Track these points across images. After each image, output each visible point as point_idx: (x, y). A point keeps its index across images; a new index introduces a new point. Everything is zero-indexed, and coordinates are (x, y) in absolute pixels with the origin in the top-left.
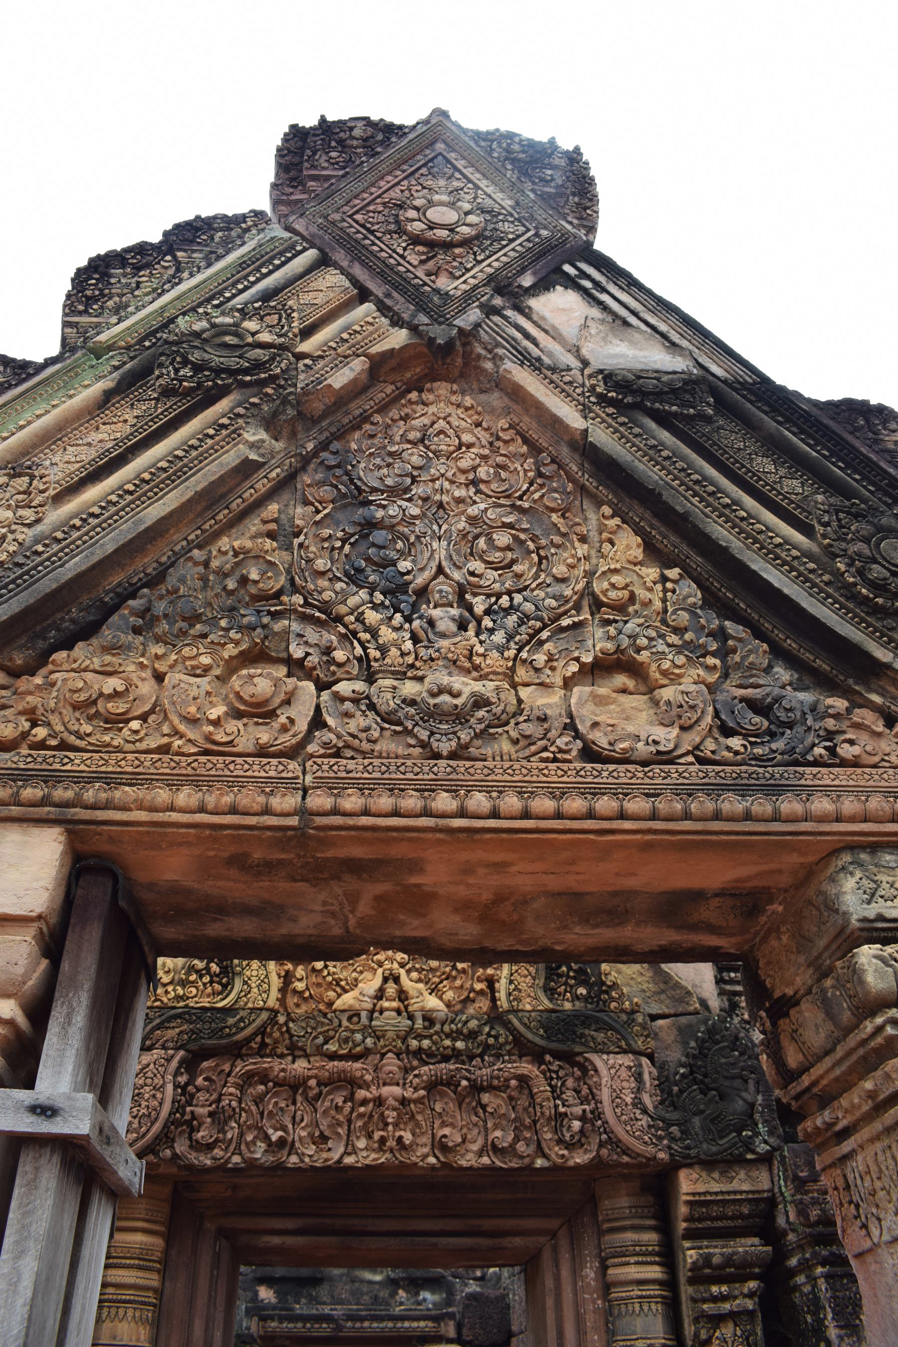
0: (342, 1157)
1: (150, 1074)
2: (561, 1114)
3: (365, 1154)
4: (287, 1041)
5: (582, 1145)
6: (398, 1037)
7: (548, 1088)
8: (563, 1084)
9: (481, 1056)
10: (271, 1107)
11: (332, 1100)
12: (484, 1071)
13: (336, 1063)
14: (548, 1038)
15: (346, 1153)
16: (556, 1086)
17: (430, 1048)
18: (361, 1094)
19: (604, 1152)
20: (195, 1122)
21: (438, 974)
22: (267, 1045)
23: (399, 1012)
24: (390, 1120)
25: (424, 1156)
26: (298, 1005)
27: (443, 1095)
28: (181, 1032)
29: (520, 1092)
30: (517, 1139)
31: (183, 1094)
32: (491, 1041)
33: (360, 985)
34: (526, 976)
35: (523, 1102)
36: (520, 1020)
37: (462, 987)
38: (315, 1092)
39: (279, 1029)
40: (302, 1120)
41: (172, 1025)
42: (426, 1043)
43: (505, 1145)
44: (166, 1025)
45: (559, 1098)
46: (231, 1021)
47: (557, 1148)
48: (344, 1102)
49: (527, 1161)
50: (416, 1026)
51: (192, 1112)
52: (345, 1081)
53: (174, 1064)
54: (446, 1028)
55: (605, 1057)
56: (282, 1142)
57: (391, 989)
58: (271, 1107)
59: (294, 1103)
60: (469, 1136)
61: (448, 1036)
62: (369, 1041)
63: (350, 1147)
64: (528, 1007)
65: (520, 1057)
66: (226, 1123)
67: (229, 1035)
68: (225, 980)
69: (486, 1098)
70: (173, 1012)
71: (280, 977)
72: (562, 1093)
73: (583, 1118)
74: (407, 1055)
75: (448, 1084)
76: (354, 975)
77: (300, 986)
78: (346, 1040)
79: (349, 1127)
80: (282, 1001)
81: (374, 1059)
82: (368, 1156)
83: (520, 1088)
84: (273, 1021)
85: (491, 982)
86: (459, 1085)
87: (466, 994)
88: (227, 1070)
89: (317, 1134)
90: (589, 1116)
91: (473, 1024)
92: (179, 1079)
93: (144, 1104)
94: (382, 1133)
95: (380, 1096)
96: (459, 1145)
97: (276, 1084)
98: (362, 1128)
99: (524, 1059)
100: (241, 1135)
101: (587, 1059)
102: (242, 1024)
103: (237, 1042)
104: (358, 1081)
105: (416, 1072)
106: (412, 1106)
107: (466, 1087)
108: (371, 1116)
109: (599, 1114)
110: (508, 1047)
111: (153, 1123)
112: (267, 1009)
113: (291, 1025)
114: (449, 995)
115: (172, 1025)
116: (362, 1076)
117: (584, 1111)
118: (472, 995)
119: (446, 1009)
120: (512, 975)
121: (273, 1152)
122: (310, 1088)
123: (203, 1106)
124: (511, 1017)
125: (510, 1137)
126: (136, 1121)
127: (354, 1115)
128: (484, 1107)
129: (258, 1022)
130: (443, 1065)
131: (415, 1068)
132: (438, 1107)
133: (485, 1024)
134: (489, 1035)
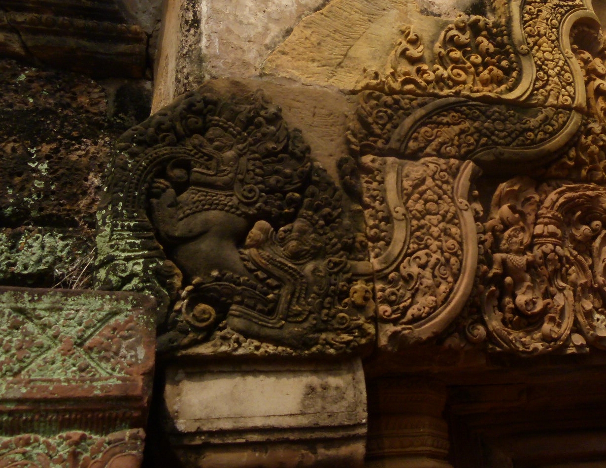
1: (429, 195)
20: (508, 279)
28: (462, 132)
51: (504, 262)
67: (533, 142)
93: (434, 245)
111: (456, 277)
115: (445, 120)
126: (428, 273)
129: (571, 127)
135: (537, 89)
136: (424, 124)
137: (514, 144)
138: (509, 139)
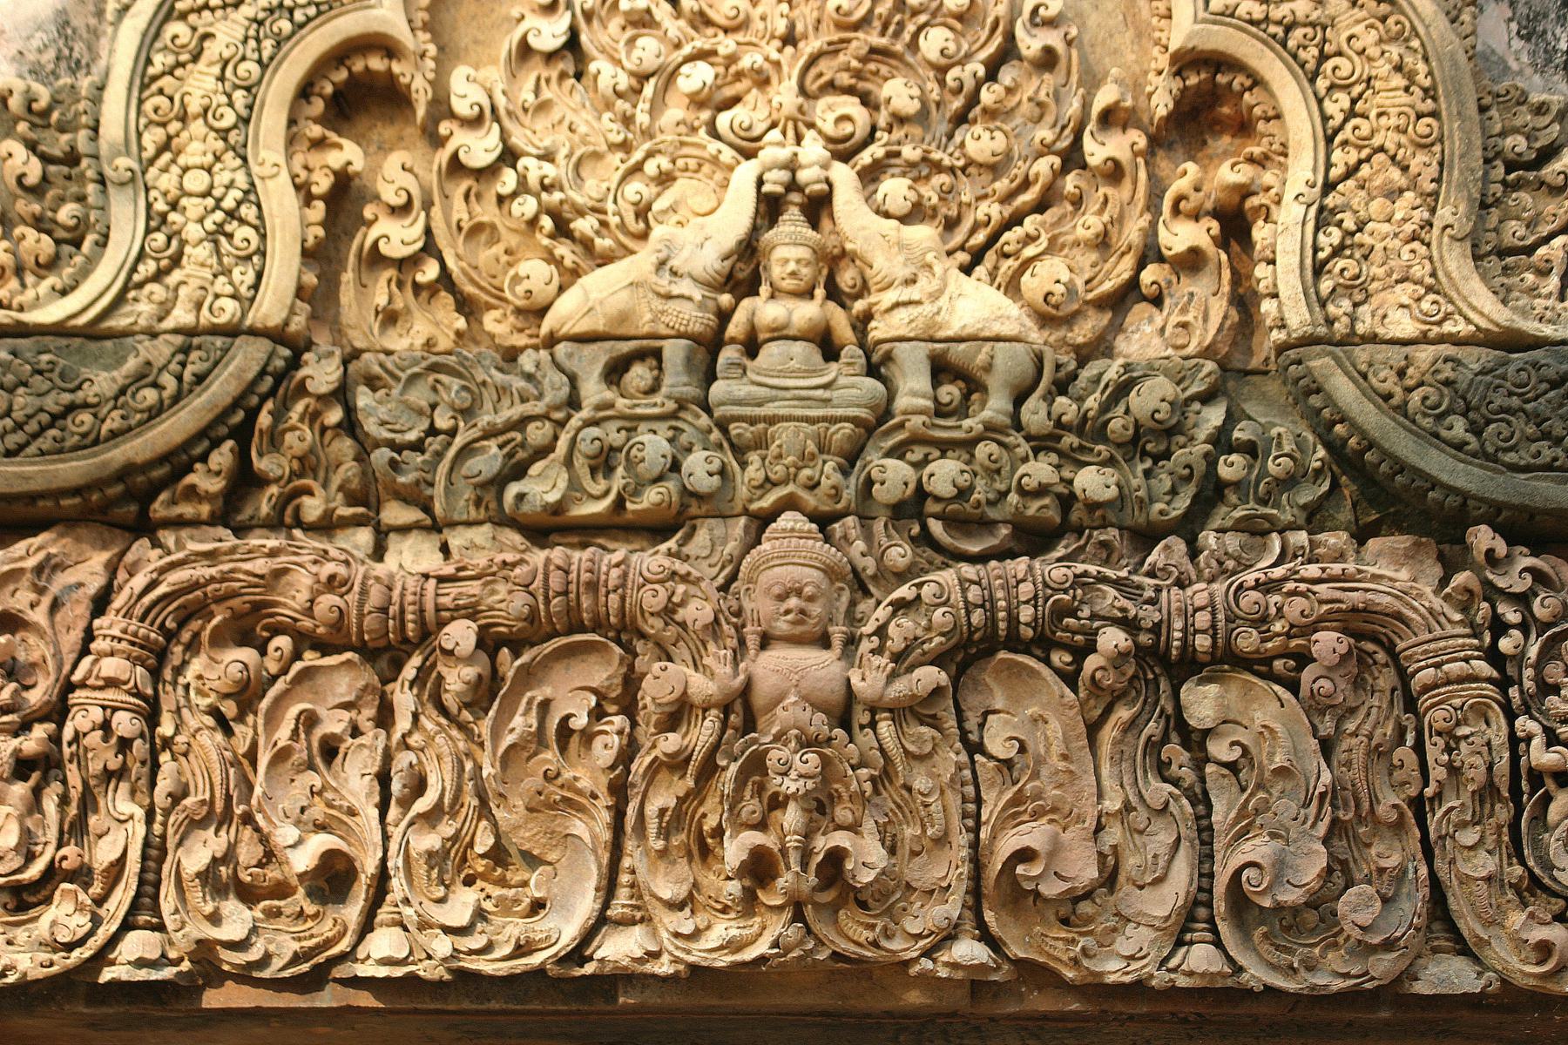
0: (589, 935)
2: (1536, 777)
4: (348, 470)
6: (823, 448)
7: (1483, 667)
9: (1189, 527)
10: (283, 735)
11: (545, 705)
12: (1199, 593)
13: (557, 554)
14: (1487, 457)
15: (601, 922)
16: (1519, 658)
17: (963, 493)
18: (662, 681)
21: (1002, 185)
22: (262, 482)
23: (829, 348)
24: (790, 785)
26: (390, 318)
29: (1358, 683)
30: (1339, 873)
32: (1231, 467)
33: (658, 232)
34: (1394, 194)
35: (1374, 718)
37: (1102, 243)
38: (470, 672)
39: (313, 417)
40: (419, 786)
42: (945, 473)
43: (1290, 896)
47: (1516, 919)
48: (598, 714)
49: (1383, 966)
50: (902, 402)
52: (598, 625)
54: (1035, 413)
56: (332, 878)
57: (789, 248)
59: (385, 717)
60: (1131, 863)
61: (1042, 444)
62: (699, 468)
63: (623, 896)
64: (1404, 326)
65: (1361, 536)
68: (67, 213)
69: (1202, 702)
71: (309, 200)
74: (865, 519)
75: (1042, 645)
76: (635, 189)
77: (398, 237)
78: (603, 462)
79: (619, 814)
80: (319, 297)
81: (712, 541)
82: (696, 935)
83: (1357, 666)
84: (280, 382)
85: (1235, 222)
86: (1091, 648)
87: (1123, 270)
88: (95, 584)
91: (1149, 398)
94: (754, 838)
95: (747, 690)
96: (1088, 895)
97: (304, 641)
98: (674, 820)
99: (1373, 544)
100: (154, 852)
102: (150, 396)
103: (127, 471)
104: (653, 626)
105: (905, 591)
106: (885, 728)
107: (1120, 658)
108: (709, 769)
110: (1307, 495)
112: (253, 332)
113: (364, 399)
114: (1048, 276)
116: (669, 611)
118: (1149, 275)
119: (1036, 336)
120: (1329, 187)
124: (1320, 363)
125: (1311, 866)
127: (640, 765)
128: (1195, 740)
129: (222, 387)
130: (1020, 565)
131: (902, 577)
132: (998, 742)
133: (1207, 398)
134: (1222, 441)
135: (140, 286)
137: (32, 449)
138: (19, 437)
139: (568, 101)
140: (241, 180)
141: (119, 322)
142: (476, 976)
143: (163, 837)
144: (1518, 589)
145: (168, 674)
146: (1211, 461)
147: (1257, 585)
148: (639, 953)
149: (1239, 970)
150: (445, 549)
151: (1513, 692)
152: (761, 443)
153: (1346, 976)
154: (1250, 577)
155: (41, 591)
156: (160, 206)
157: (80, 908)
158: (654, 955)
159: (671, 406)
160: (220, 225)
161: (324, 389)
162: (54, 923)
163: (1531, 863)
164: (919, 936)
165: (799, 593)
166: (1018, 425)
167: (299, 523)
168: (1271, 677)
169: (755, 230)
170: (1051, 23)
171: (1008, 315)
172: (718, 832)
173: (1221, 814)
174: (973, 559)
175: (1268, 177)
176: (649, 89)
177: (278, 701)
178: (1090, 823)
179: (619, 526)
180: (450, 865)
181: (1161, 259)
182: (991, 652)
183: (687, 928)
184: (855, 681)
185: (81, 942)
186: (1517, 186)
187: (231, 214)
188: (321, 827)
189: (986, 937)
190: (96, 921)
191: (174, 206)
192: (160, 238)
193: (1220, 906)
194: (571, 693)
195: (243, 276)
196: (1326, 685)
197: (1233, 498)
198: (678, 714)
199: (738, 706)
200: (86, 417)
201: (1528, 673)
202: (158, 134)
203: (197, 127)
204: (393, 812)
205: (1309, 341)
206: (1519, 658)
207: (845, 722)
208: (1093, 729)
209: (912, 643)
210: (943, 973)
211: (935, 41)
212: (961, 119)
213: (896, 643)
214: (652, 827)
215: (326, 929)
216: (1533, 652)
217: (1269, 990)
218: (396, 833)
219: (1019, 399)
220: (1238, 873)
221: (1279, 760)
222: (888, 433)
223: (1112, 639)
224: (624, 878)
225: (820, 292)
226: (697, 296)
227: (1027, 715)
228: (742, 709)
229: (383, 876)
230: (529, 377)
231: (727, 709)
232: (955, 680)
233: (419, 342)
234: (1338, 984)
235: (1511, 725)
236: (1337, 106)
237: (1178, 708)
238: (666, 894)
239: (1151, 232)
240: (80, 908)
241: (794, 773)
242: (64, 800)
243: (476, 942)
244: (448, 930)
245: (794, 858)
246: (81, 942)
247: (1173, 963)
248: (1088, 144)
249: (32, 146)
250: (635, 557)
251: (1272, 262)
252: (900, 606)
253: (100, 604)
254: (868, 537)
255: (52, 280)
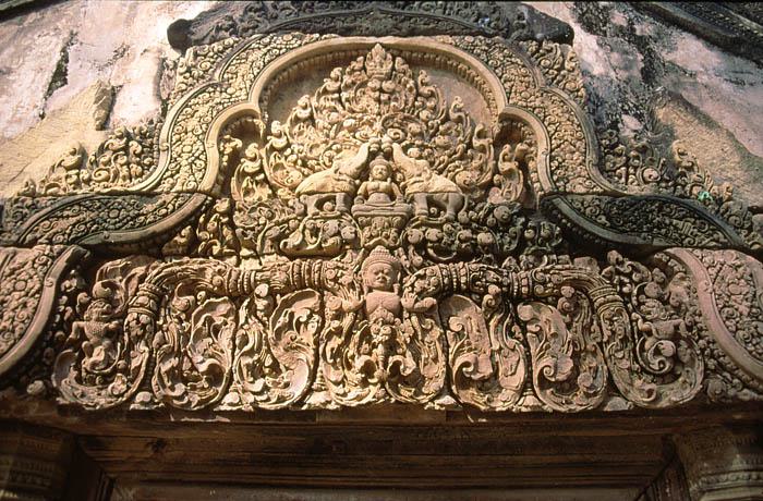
1: (24, 276)
2: (640, 333)
3: (340, 390)
5: (677, 377)
8: (641, 291)
9: (516, 254)
10: (199, 324)
11: (292, 315)
12: (523, 274)
14: (613, 227)
15: (309, 391)
19: (715, 384)
23: (392, 196)
25: (433, 398)
26: (248, 192)
27: (462, 306)
28: (78, 222)
31: (72, 302)
32: (528, 234)
36: (570, 204)
37: (481, 169)
38: (265, 302)
41: (66, 213)
42: (433, 234)
43: (560, 377)
44: (59, 214)
45: (637, 308)
46: (149, 207)
47: (638, 383)
48: (310, 317)
53: (61, 263)
54: (462, 215)
55: (698, 252)
56: (215, 374)
57: (378, 166)
58: (199, 324)
61: (466, 226)
62: (347, 232)
66: (131, 346)
69: (525, 311)
70: (72, 198)
72: (640, 304)
73: (675, 337)
75: (468, 292)
78: (315, 232)
79: (316, 350)
80: (223, 187)
82: (345, 395)
84: (209, 209)
86: (486, 292)
87: (488, 177)
89: (269, 362)
90: (683, 332)
91: (499, 213)
92: (67, 283)
94: (365, 358)
96: (488, 380)
97: (210, 294)
98: (337, 353)
99: (576, 260)
100: (151, 363)
101: (673, 257)
102: (164, 211)
103: (154, 235)
104: (330, 284)
105: (421, 272)
107: (496, 296)
108: (349, 335)
109: (701, 330)
112: (200, 192)
115: (66, 213)
116: (335, 279)
117: (677, 327)
118: (496, 177)
120: (552, 151)
121: (203, 389)
122: (258, 296)
123: (98, 320)
125: (567, 366)
127: (325, 332)
128: (523, 326)
129: (188, 208)
133: (519, 215)
134: (525, 225)
136: (47, 219)
138: (120, 224)
139: (309, 131)
140: (201, 148)
141: (159, 190)
142: (264, 410)
143: (155, 359)
144: (628, 271)
145: (163, 304)
146: (522, 231)
147: (542, 271)
148: (323, 401)
149: (544, 404)
150: (260, 264)
151: (629, 305)
152: (369, 224)
153: (581, 405)
154: (539, 269)
155: (124, 277)
156: (175, 156)
157: (123, 382)
158: (330, 402)
159: (339, 213)
160: (193, 162)
161: (222, 210)
162: (113, 388)
163: (641, 363)
164: (427, 395)
165: (383, 272)
166: (456, 219)
167: (212, 255)
168: (547, 303)
169: (368, 162)
170: (460, 110)
171: (453, 187)
172: (353, 357)
173: (533, 350)
174: (445, 262)
175: (532, 149)
176: (334, 127)
177: (198, 313)
178: (488, 353)
179: (322, 254)
180: (256, 371)
181: (499, 173)
182: (450, 295)
183: (341, 392)
184: (403, 302)
185: (122, 395)
186: (609, 153)
187: (198, 158)
188: (211, 357)
189: (452, 395)
190: (128, 388)
191: (179, 156)
192: (174, 165)
193: (536, 382)
194: (301, 310)
195: (198, 175)
196: (567, 304)
197: (529, 243)
198: (339, 315)
199: (360, 312)
200: (143, 218)
201: (634, 299)
202: (178, 136)
203: (190, 134)
204: (237, 351)
205: (551, 194)
206: (629, 295)
207: (400, 316)
208: (487, 322)
209: (424, 289)
210: (437, 408)
211: (424, 114)
212: (434, 135)
213: (417, 289)
214: (328, 355)
215: (211, 393)
216: (635, 292)
217: (555, 412)
218: (236, 358)
219: (457, 212)
220: (542, 370)
221: (553, 331)
222: (413, 222)
223: (493, 289)
224: (319, 374)
225: (389, 179)
226: (348, 180)
227: (466, 318)
228: (361, 312)
229: (231, 373)
230: (292, 207)
231: (356, 312)
232: (439, 303)
233: (256, 198)
234: (579, 408)
235: (630, 316)
236: (552, 129)
237: (517, 314)
238: (333, 379)
239: (496, 165)
240: (123, 382)
241: (381, 334)
242: (122, 348)
243: (264, 397)
244: (254, 393)
245: (381, 364)
246: (122, 395)
247: (520, 403)
248: (474, 141)
249: (140, 143)
250: (324, 262)
251: (536, 172)
252: (419, 277)
253: (142, 280)
254: (407, 254)
255: (140, 179)
